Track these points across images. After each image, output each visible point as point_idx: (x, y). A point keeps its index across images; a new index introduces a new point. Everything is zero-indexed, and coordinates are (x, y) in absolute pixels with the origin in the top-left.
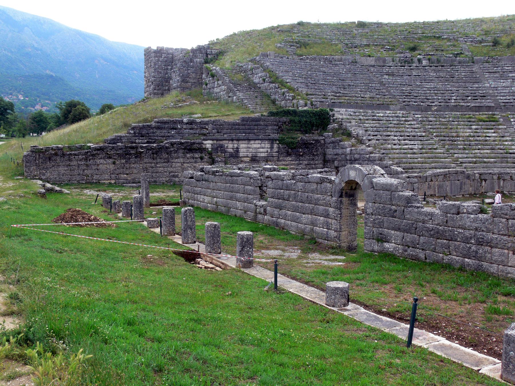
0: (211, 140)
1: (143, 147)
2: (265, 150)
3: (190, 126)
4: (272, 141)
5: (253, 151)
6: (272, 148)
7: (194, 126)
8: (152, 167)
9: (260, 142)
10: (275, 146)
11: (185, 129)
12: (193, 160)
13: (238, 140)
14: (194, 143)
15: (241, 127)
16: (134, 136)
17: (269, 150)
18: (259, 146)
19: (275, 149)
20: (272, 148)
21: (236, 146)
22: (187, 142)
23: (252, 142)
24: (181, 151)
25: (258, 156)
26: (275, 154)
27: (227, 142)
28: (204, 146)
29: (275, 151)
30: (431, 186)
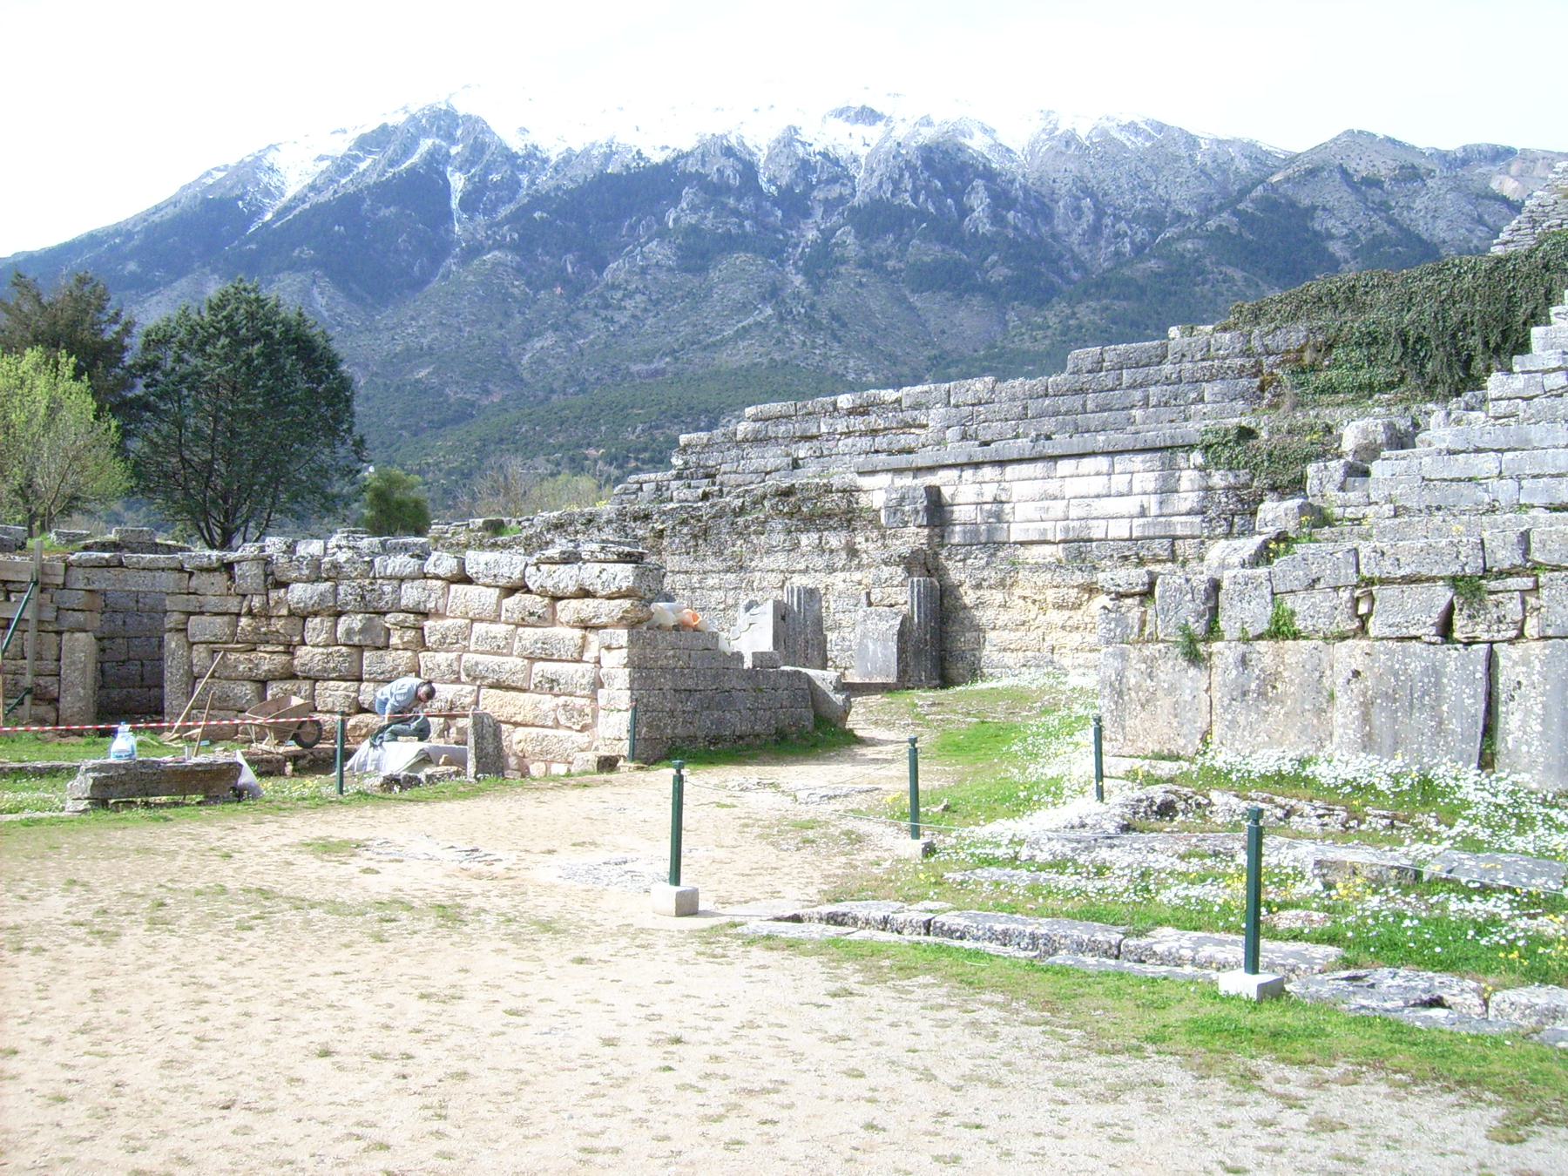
0: (888, 471)
1: (665, 513)
2: (1131, 505)
3: (858, 423)
4: (1167, 450)
5: (1073, 514)
6: (1167, 489)
7: (874, 420)
8: (693, 590)
9: (1102, 463)
10: (1188, 479)
11: (848, 434)
12: (820, 562)
13: (1002, 463)
14: (828, 489)
15: (1064, 403)
16: (679, 477)
17: (1152, 503)
18: (1099, 484)
19: (1187, 498)
20: (1167, 489)
21: (990, 492)
22: (805, 488)
23: (1065, 467)
24: (777, 524)
25: (1097, 533)
26: (1181, 525)
27: (955, 473)
28: (864, 500)
29: (1185, 507)
30: (1270, 680)
